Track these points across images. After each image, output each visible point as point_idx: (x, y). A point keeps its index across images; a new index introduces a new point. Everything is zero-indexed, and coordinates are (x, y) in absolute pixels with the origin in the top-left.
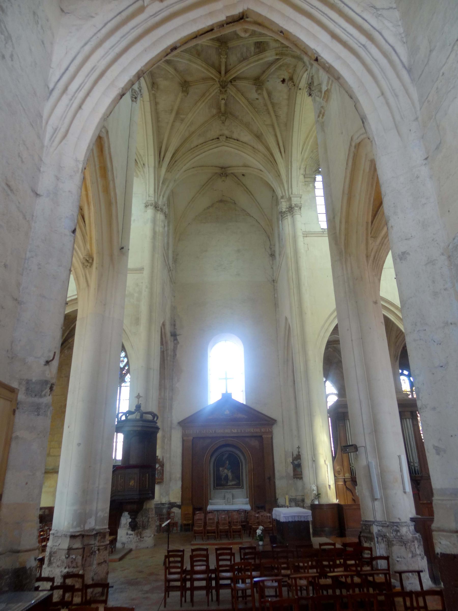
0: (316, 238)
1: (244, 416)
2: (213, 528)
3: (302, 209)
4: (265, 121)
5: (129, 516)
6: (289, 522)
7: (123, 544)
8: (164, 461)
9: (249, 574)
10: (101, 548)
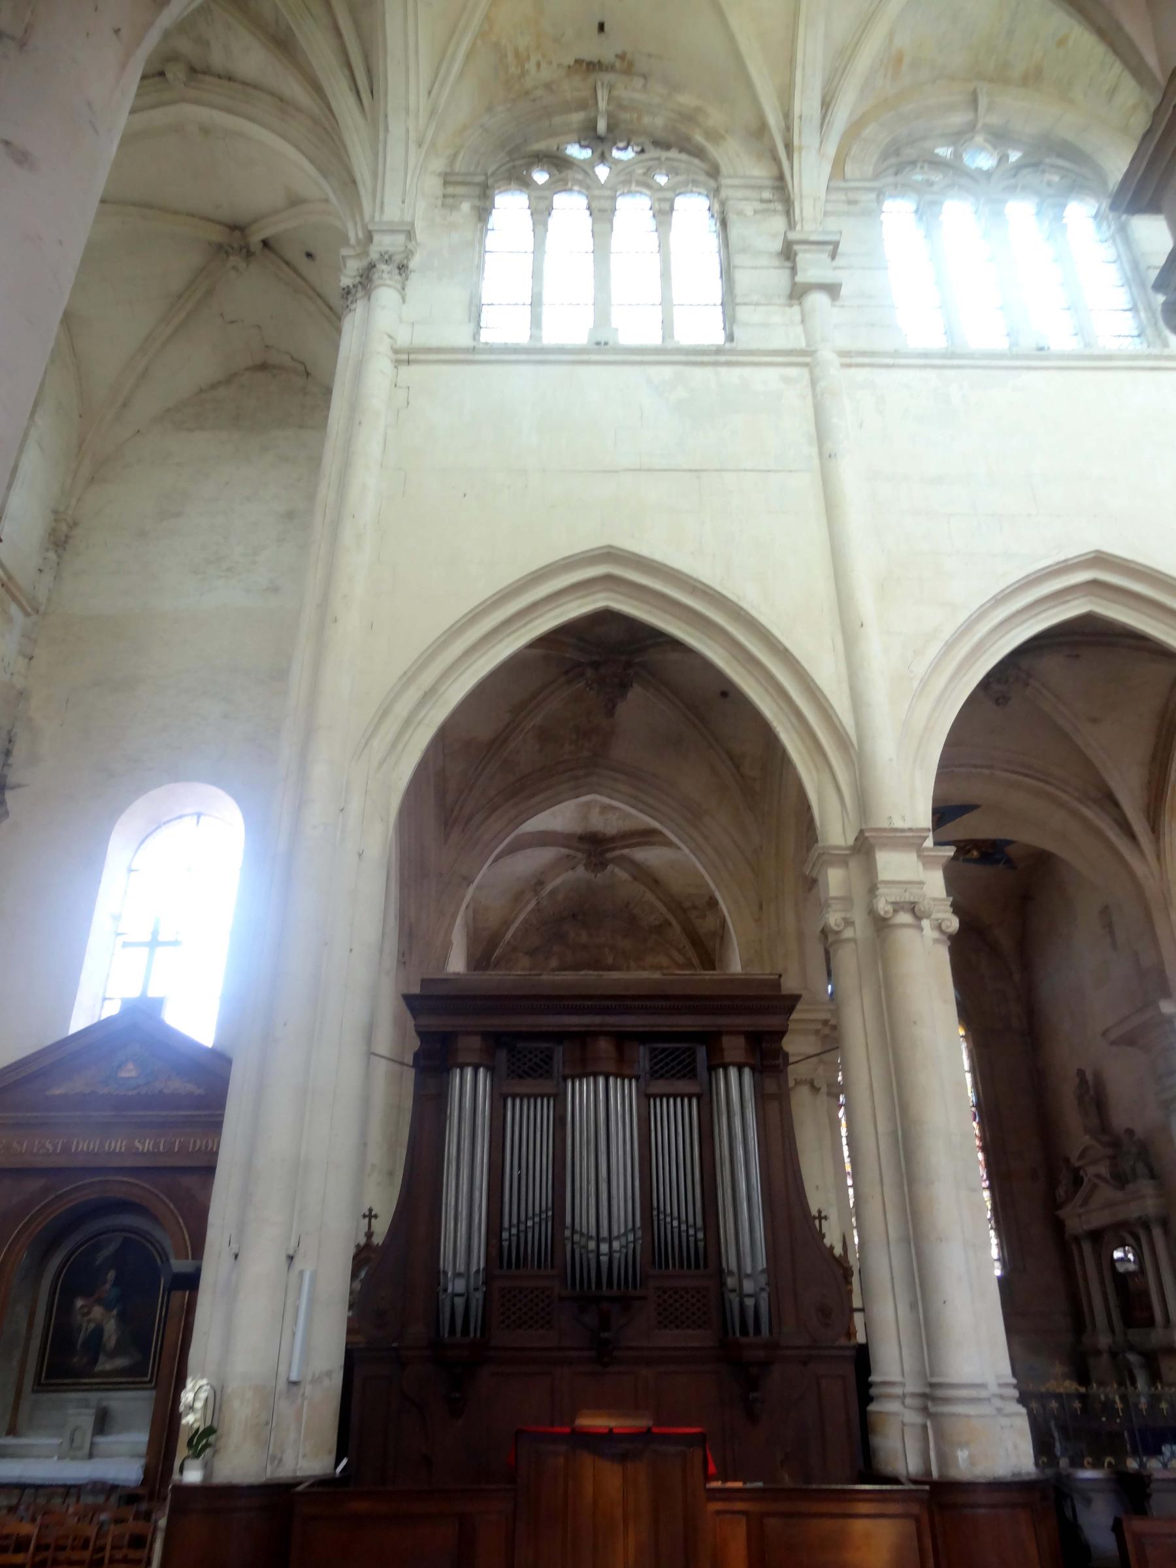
1: (191, 1087)
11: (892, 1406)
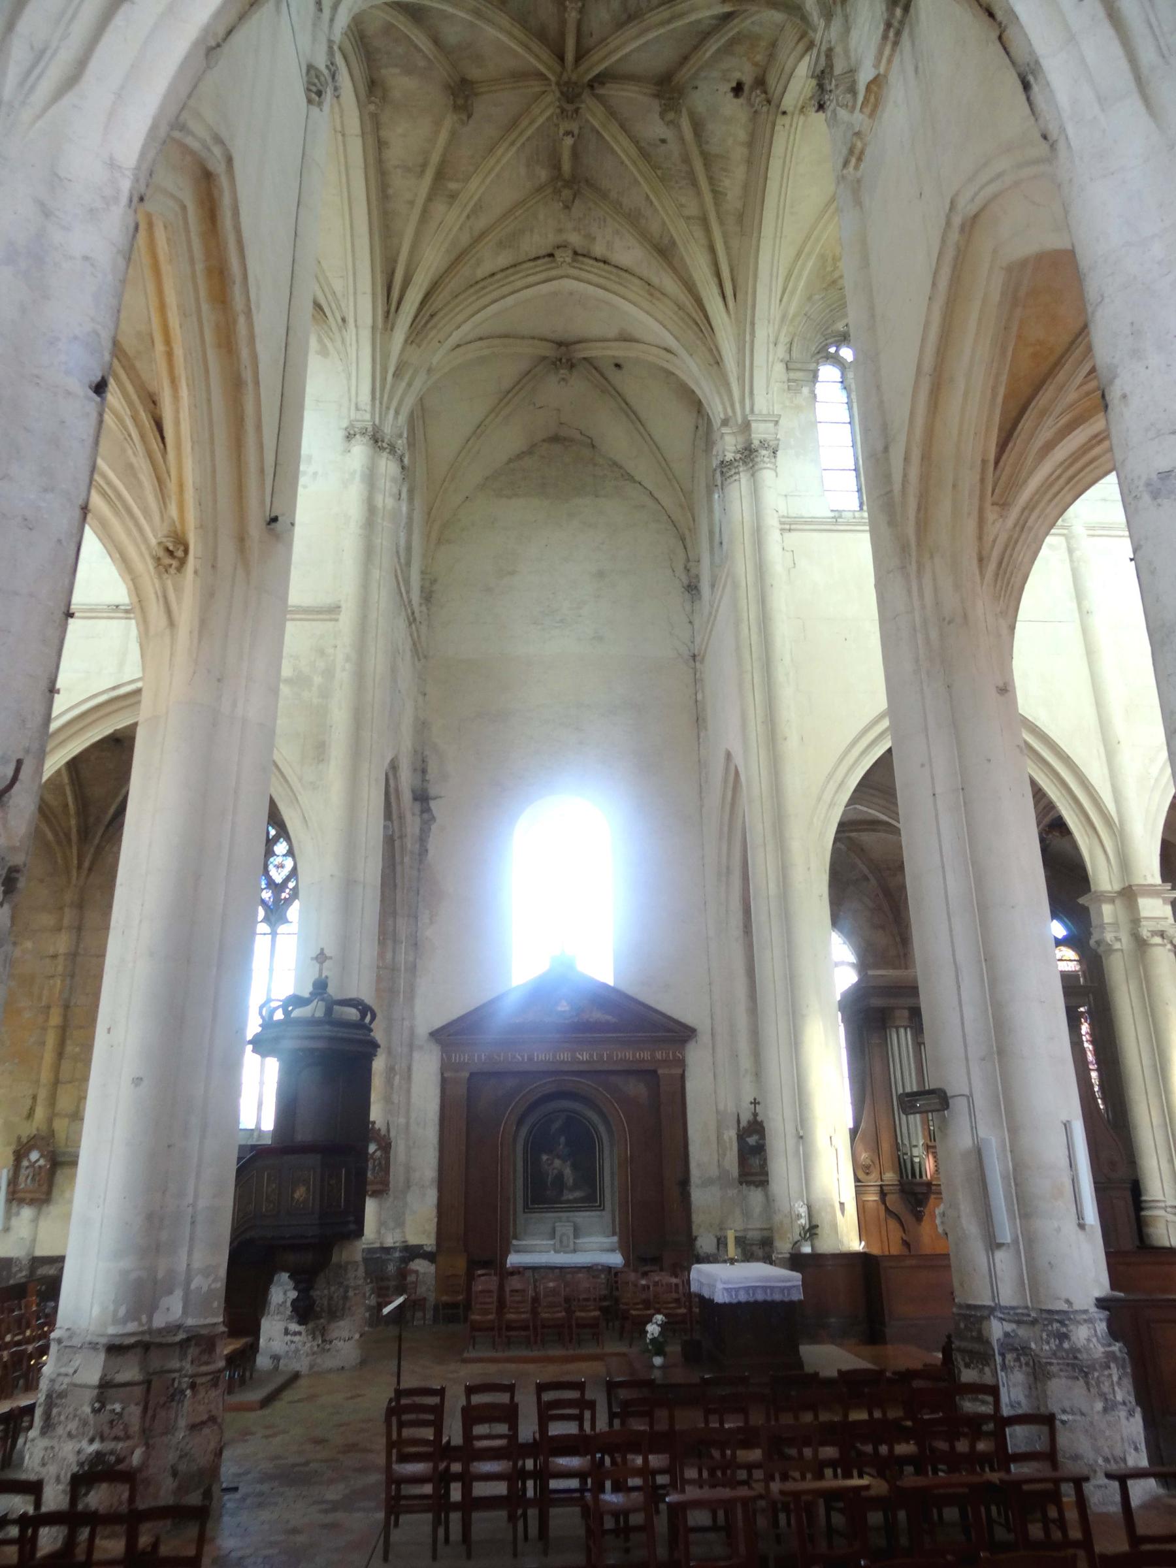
0: (815, 534)
1: (609, 1018)
2: (523, 1316)
3: (778, 453)
4: (682, 206)
5: (291, 1284)
6: (739, 1303)
7: (276, 1358)
8: (392, 1134)
9: (639, 1461)
10: (199, 1380)
11: (1161, 1213)
